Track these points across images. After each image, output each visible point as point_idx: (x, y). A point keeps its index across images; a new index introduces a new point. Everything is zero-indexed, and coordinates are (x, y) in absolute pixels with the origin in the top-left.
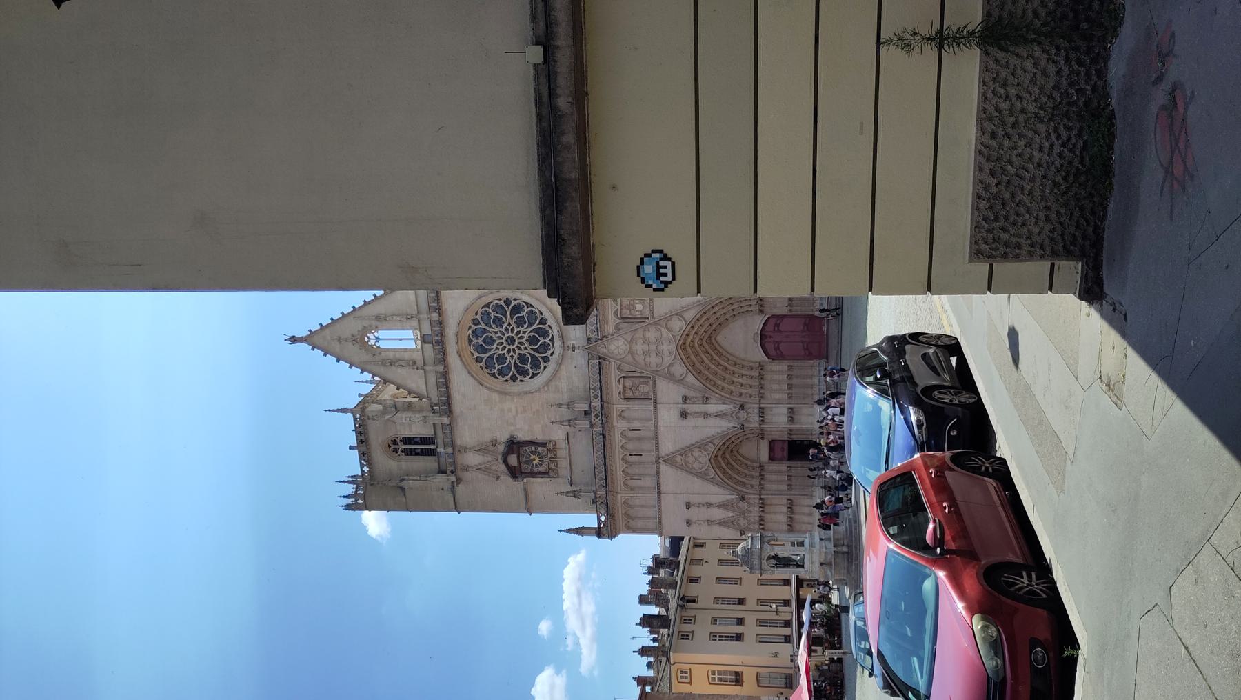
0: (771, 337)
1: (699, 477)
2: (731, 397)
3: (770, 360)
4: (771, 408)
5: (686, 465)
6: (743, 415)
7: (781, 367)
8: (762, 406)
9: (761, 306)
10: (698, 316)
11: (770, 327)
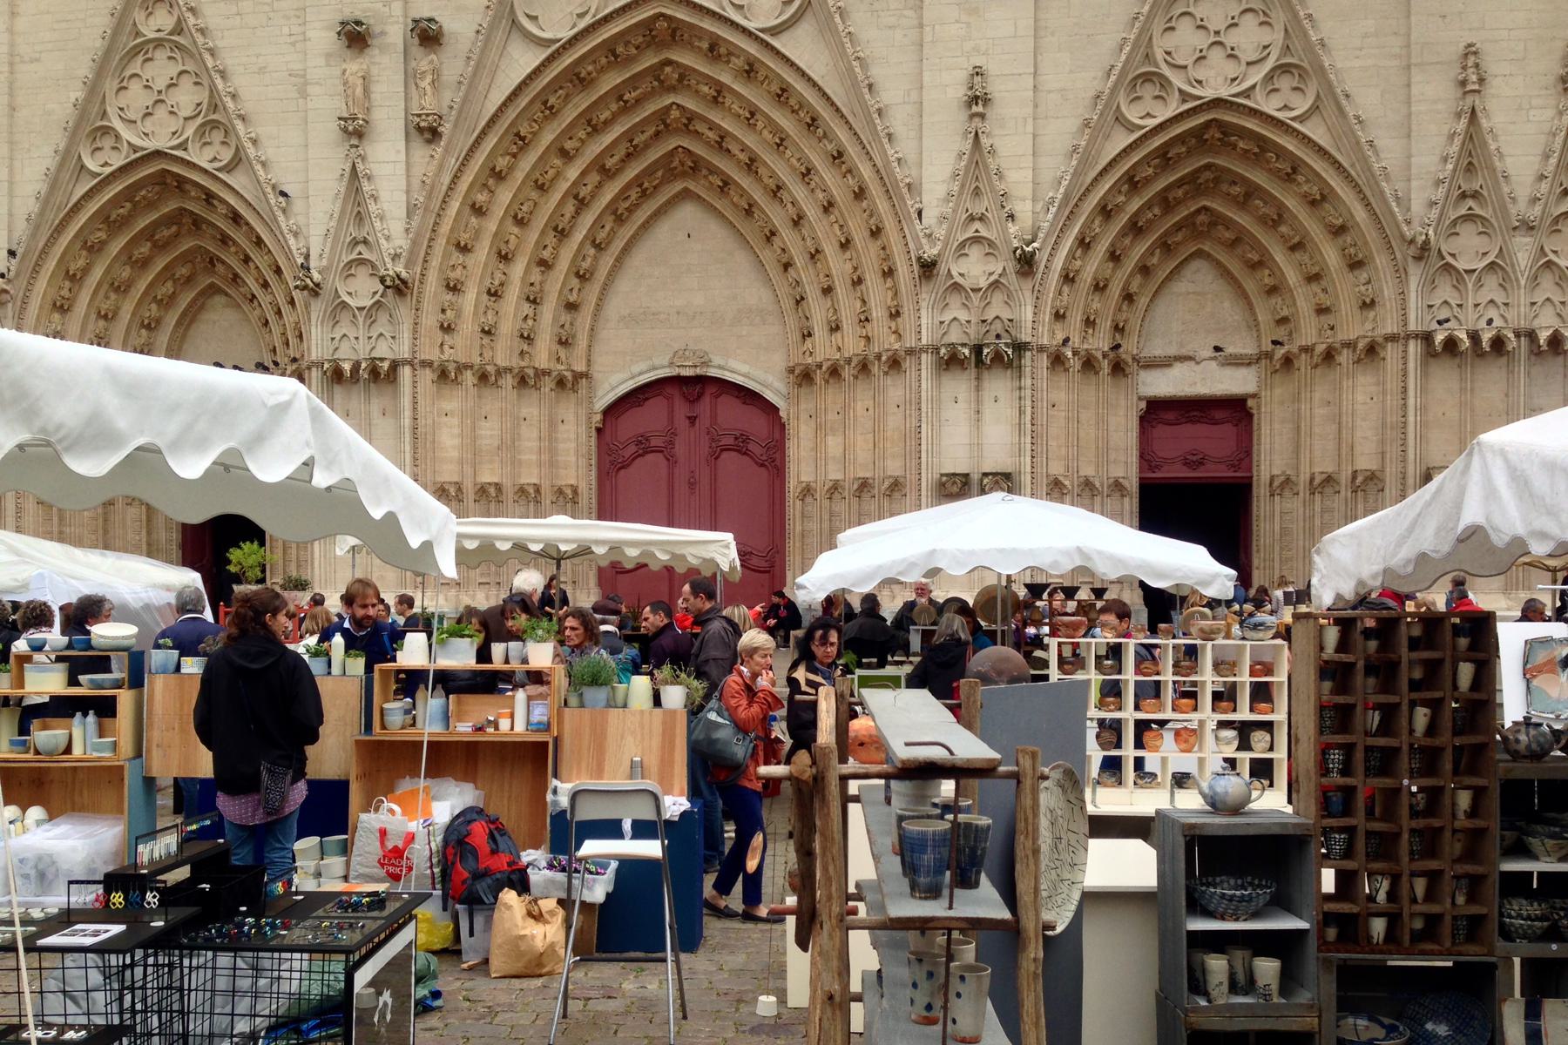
0: (692, 420)
1: (82, 109)
2: (440, 244)
3: (598, 417)
4: (397, 414)
5: (135, 52)
6: (362, 291)
7: (574, 459)
8: (406, 372)
9: (835, 372)
10: (799, 85)
11: (732, 415)
